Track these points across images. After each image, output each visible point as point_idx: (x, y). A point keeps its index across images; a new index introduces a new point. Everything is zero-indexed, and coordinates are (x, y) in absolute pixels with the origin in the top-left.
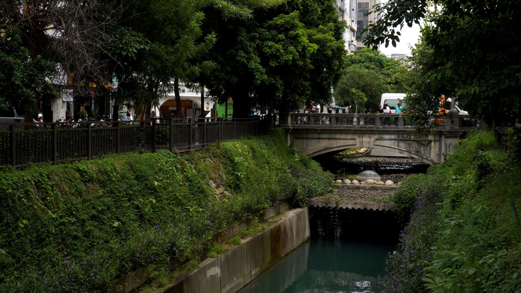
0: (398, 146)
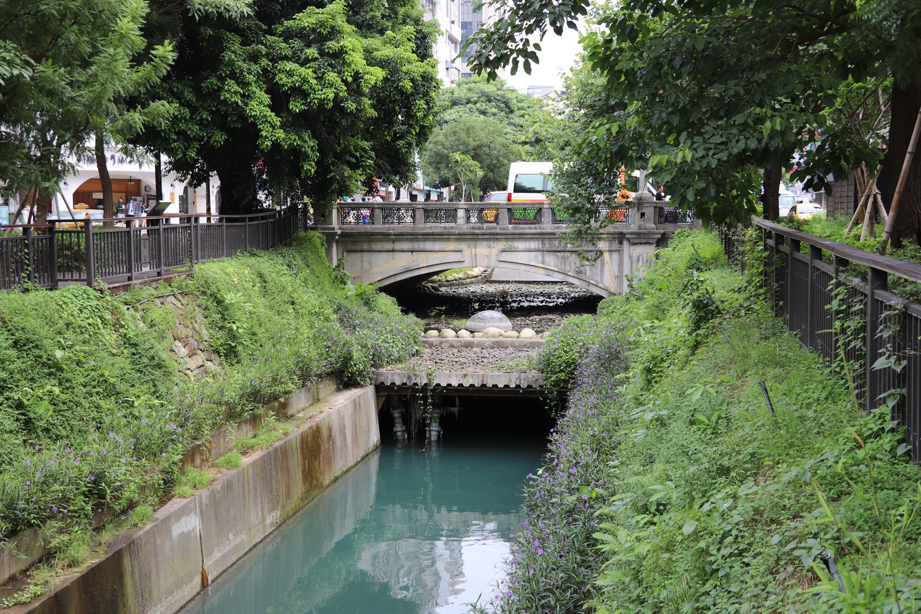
0: (543, 262)
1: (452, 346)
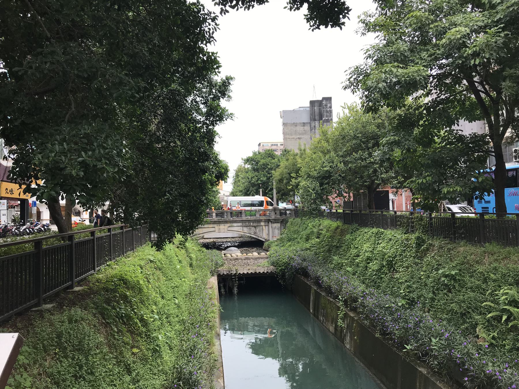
1: (231, 260)
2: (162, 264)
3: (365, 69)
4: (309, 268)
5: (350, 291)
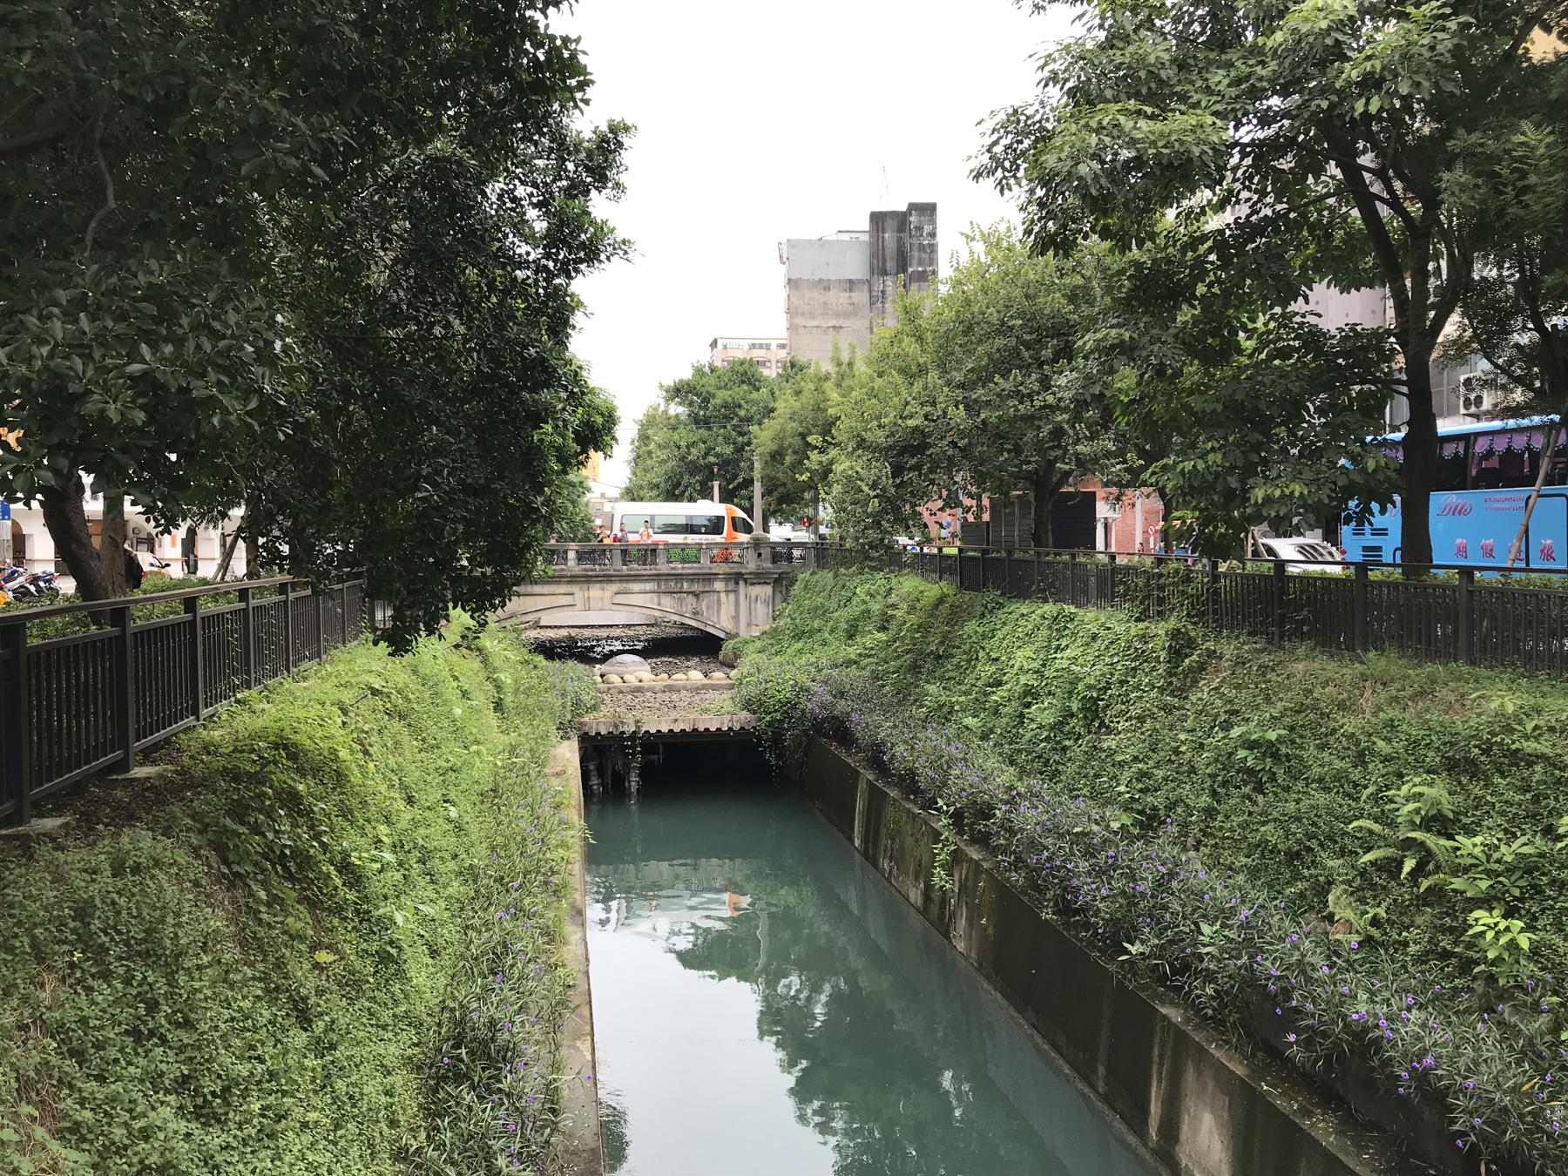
0: (659, 604)
1: (621, 692)
2: (408, 700)
3: (1038, 117)
4: (855, 717)
5: (971, 786)
